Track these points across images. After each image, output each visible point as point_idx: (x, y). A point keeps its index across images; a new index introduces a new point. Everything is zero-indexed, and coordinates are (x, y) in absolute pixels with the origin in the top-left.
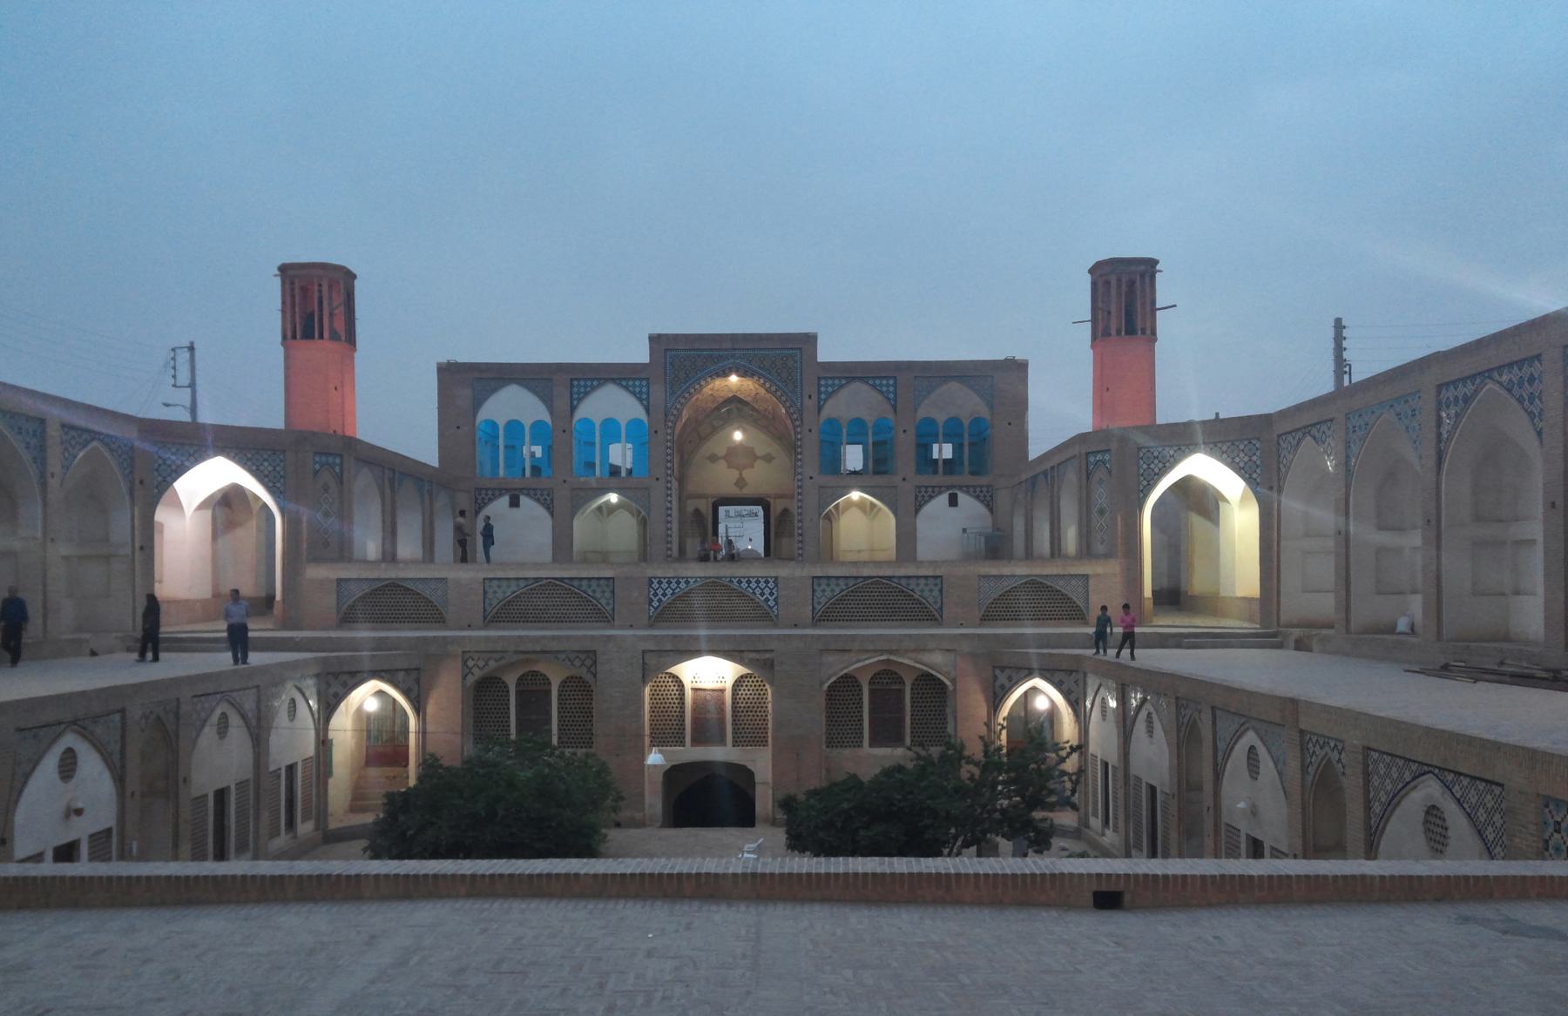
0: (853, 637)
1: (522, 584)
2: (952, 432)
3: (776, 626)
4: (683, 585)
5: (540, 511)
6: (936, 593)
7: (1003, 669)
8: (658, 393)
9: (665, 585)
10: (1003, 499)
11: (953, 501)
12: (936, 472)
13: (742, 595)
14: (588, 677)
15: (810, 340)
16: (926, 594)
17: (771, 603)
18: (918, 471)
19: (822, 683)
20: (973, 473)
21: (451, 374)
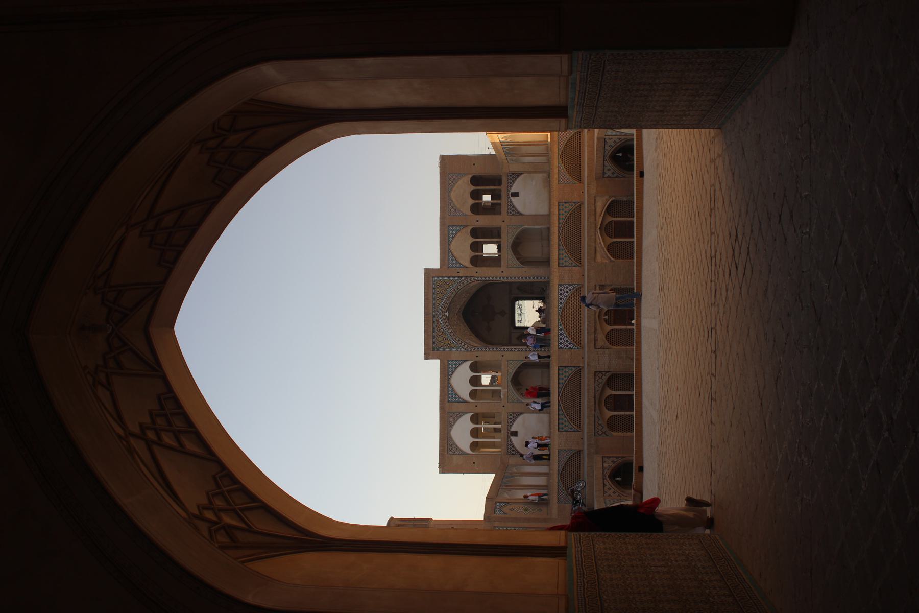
0: (589, 246)
1: (561, 412)
2: (476, 195)
3: (583, 285)
4: (562, 332)
5: (520, 420)
6: (567, 205)
7: (604, 173)
8: (455, 355)
9: (562, 341)
10: (514, 168)
11: (516, 195)
12: (500, 204)
13: (567, 303)
14: (608, 375)
15: (428, 273)
16: (567, 210)
17: (572, 287)
18: (500, 213)
19: (611, 261)
20: (500, 184)
21: (446, 466)
